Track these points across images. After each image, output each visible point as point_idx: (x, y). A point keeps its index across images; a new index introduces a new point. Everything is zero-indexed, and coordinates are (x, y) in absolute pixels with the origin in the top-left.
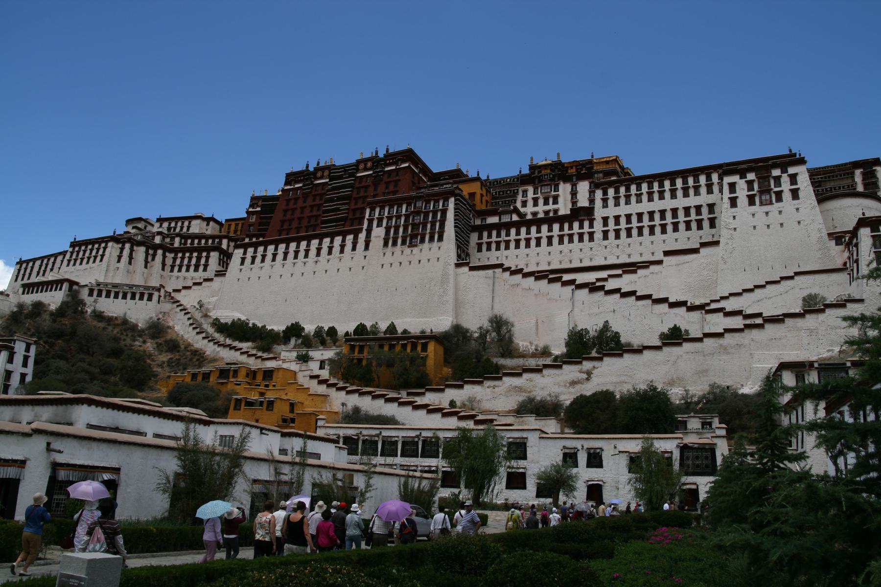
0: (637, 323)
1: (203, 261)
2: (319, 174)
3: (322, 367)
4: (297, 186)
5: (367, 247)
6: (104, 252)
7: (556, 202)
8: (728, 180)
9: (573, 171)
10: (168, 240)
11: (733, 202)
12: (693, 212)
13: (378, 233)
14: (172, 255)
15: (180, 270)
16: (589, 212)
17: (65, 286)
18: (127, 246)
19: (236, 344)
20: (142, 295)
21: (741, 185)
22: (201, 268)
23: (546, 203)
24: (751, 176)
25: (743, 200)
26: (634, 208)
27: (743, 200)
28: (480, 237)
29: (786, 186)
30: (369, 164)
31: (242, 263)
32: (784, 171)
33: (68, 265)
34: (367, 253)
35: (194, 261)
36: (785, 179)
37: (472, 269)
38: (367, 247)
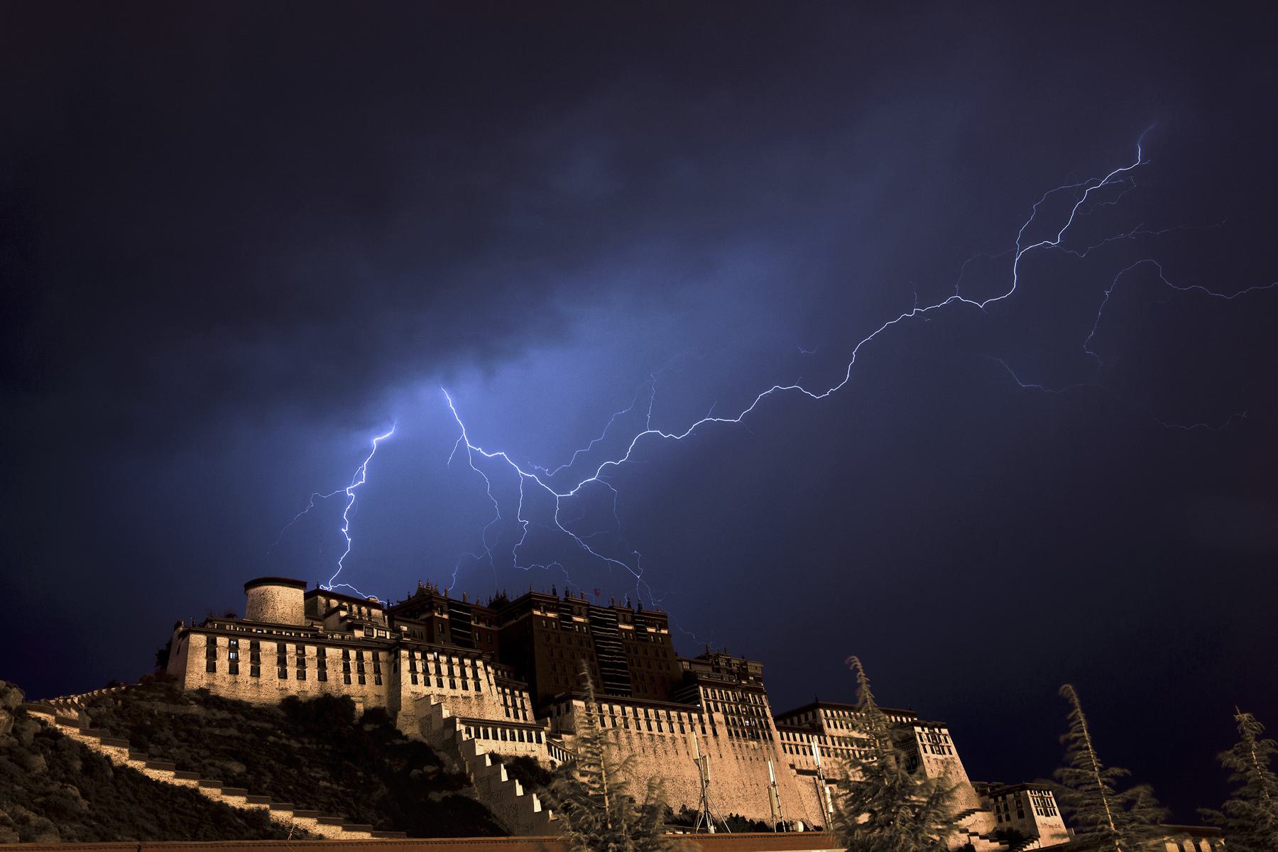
4: (550, 615)
5: (715, 734)
8: (918, 729)
13: (718, 717)
30: (629, 618)
33: (415, 681)
34: (720, 738)
37: (800, 772)
38: (715, 734)
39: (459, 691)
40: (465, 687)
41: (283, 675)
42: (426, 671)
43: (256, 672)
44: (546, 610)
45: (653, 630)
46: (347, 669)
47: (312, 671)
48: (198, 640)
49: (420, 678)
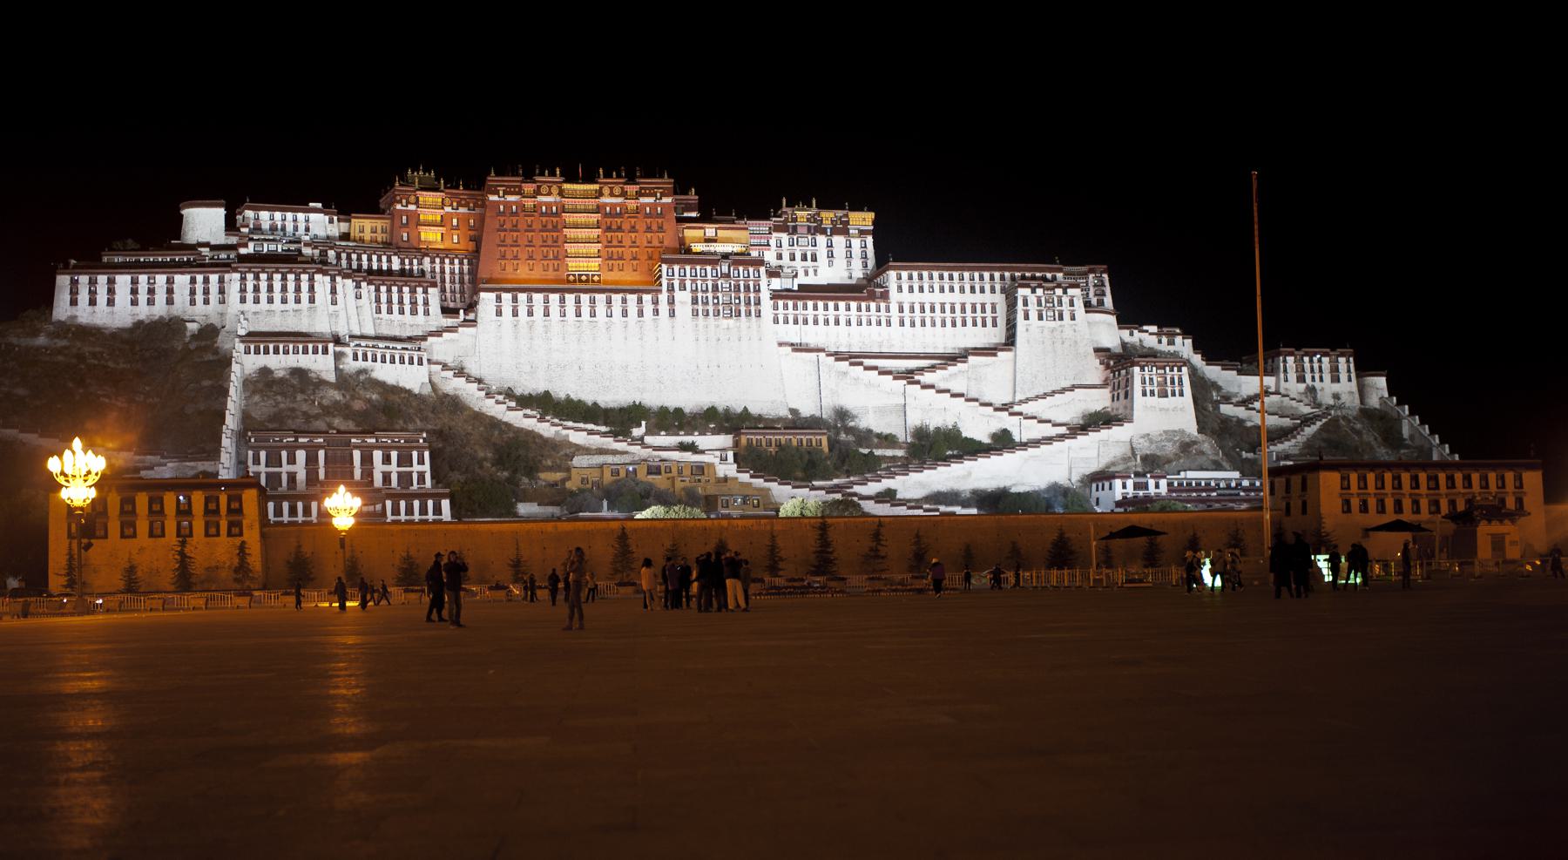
0: (978, 427)
1: (420, 301)
2: (544, 189)
3: (724, 459)
5: (672, 314)
6: (312, 289)
7: (814, 259)
8: (1022, 292)
9: (827, 224)
10: (317, 252)
11: (1027, 317)
12: (979, 307)
13: (683, 297)
14: (372, 288)
15: (390, 311)
16: (885, 296)
17: (331, 346)
18: (338, 279)
19: (570, 424)
20: (411, 359)
21: (1032, 299)
22: (421, 309)
23: (804, 258)
24: (1039, 292)
25: (1033, 315)
26: (927, 298)
27: (1033, 315)
28: (776, 308)
29: (1066, 308)
30: (617, 190)
31: (499, 313)
32: (1065, 292)
35: (407, 300)
36: (1065, 300)
38: (672, 314)
39: (291, 304)
40: (298, 301)
41: (134, 303)
42: (256, 289)
43: (111, 302)
44: (505, 193)
45: (651, 200)
46: (193, 292)
47: (161, 296)
48: (63, 281)
49: (250, 296)
